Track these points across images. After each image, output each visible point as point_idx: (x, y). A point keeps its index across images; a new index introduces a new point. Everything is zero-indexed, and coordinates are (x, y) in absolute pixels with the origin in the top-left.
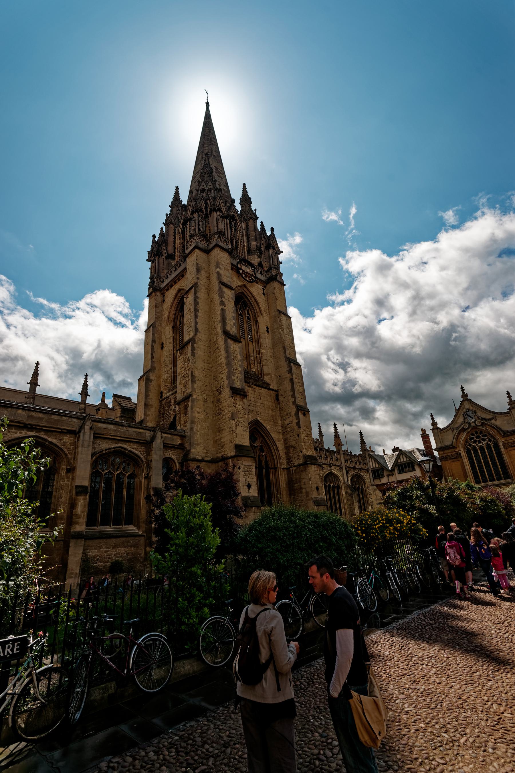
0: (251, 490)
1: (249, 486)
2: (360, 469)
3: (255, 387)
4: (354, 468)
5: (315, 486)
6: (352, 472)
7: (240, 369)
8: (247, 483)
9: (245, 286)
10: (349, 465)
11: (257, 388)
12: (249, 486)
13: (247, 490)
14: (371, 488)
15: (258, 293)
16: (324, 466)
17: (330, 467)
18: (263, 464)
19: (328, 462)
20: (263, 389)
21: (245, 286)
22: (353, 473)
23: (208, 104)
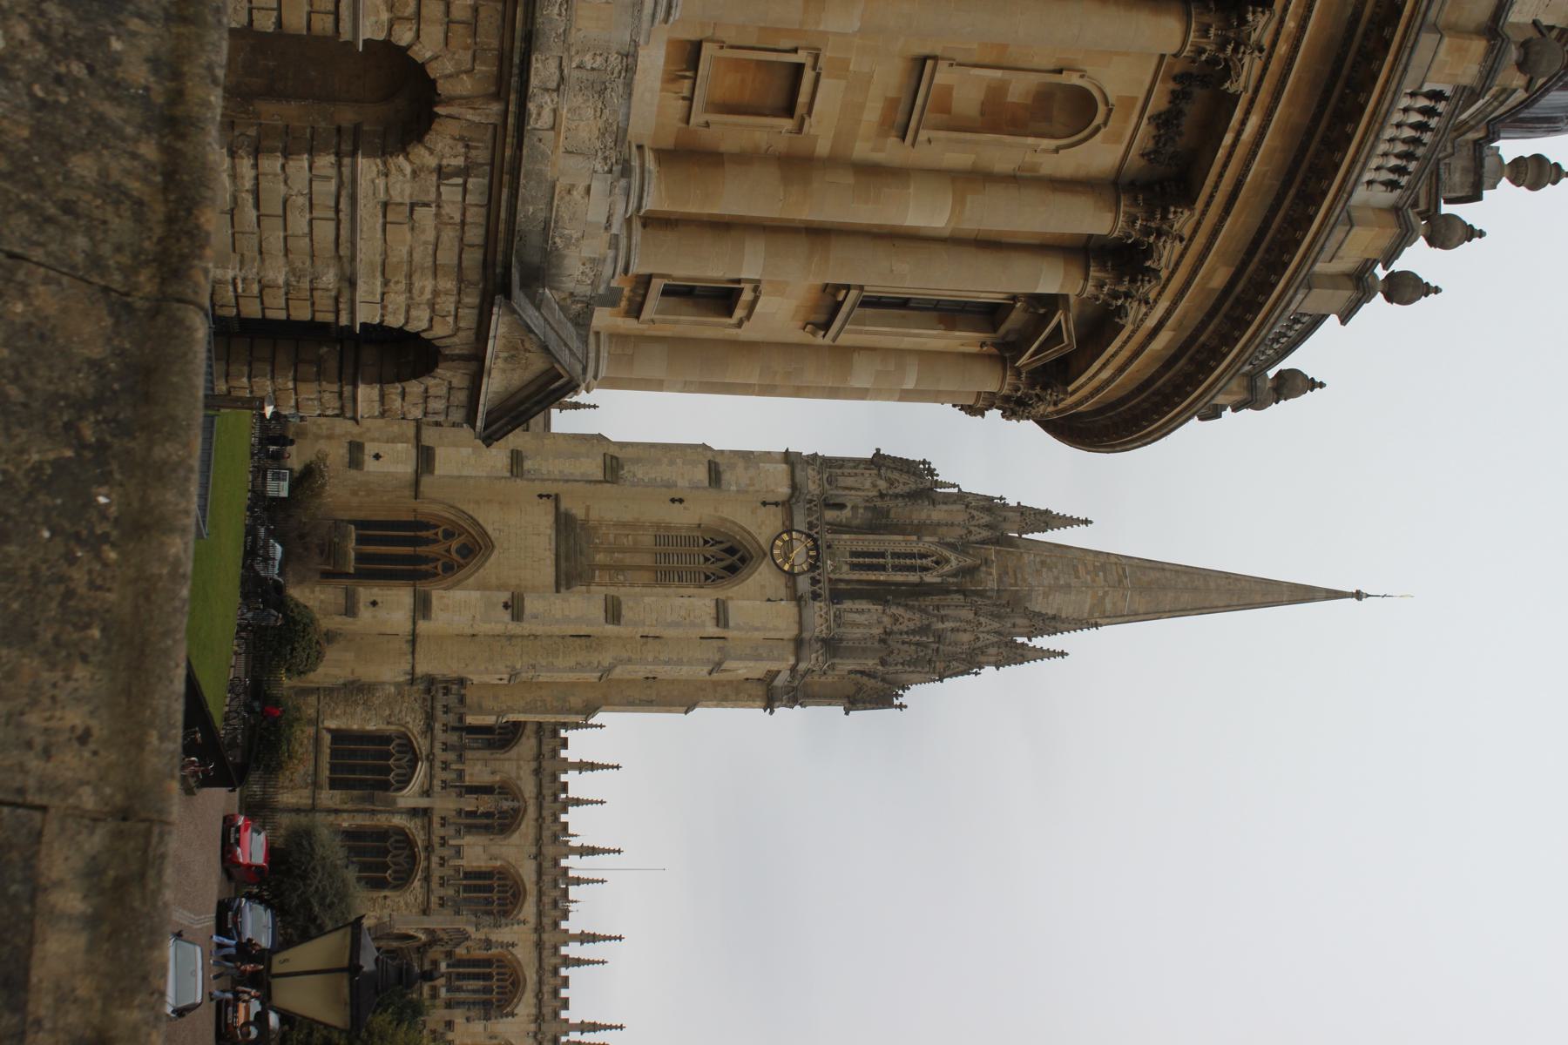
0: (372, 459)
1: (377, 457)
2: (427, 879)
3: (554, 551)
4: (429, 848)
5: (379, 600)
6: (420, 839)
7: (556, 472)
8: (381, 454)
9: (765, 554)
10: (438, 831)
11: (553, 557)
12: (377, 457)
13: (373, 453)
14: (386, 912)
15: (763, 587)
16: (429, 735)
17: (427, 757)
18: (423, 567)
19: (440, 755)
20: (553, 569)
21: (765, 554)
22: (419, 843)
23: (1358, 595)
